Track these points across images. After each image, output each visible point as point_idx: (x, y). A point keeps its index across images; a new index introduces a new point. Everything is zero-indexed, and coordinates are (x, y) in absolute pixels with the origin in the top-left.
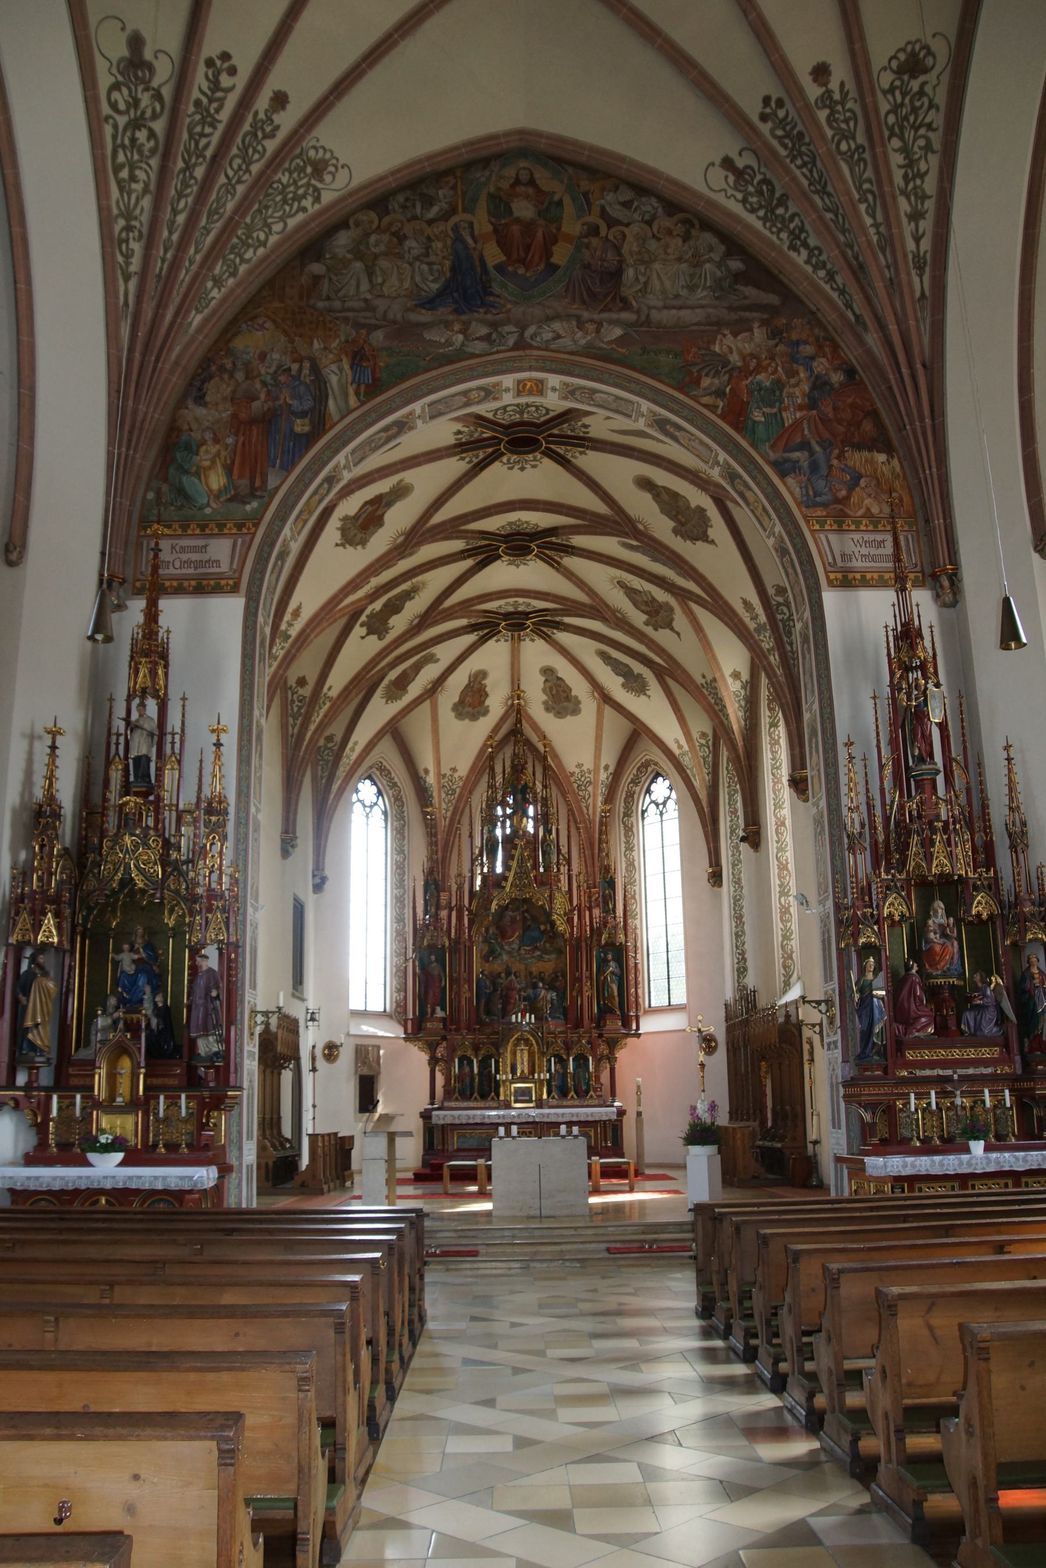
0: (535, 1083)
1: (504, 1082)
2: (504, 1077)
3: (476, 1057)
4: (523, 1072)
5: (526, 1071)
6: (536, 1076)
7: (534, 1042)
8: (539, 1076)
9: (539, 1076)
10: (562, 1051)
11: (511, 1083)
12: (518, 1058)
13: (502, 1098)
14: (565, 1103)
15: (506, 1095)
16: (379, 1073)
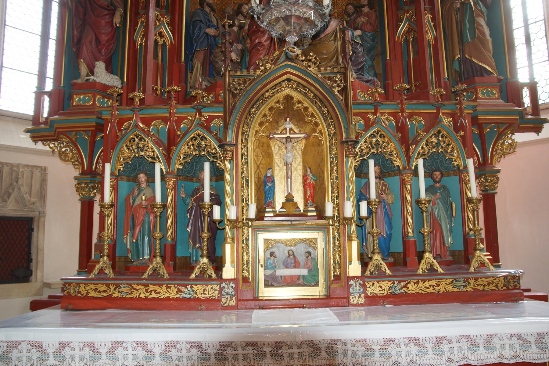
0: (326, 229)
1: (235, 223)
2: (232, 213)
3: (168, 160)
4: (289, 199)
5: (299, 199)
6: (329, 211)
7: (320, 119)
8: (339, 208)
9: (339, 208)
10: (392, 147)
11: (257, 230)
12: (277, 160)
13: (229, 272)
14: (412, 288)
15: (240, 265)
16: (42, 214)
